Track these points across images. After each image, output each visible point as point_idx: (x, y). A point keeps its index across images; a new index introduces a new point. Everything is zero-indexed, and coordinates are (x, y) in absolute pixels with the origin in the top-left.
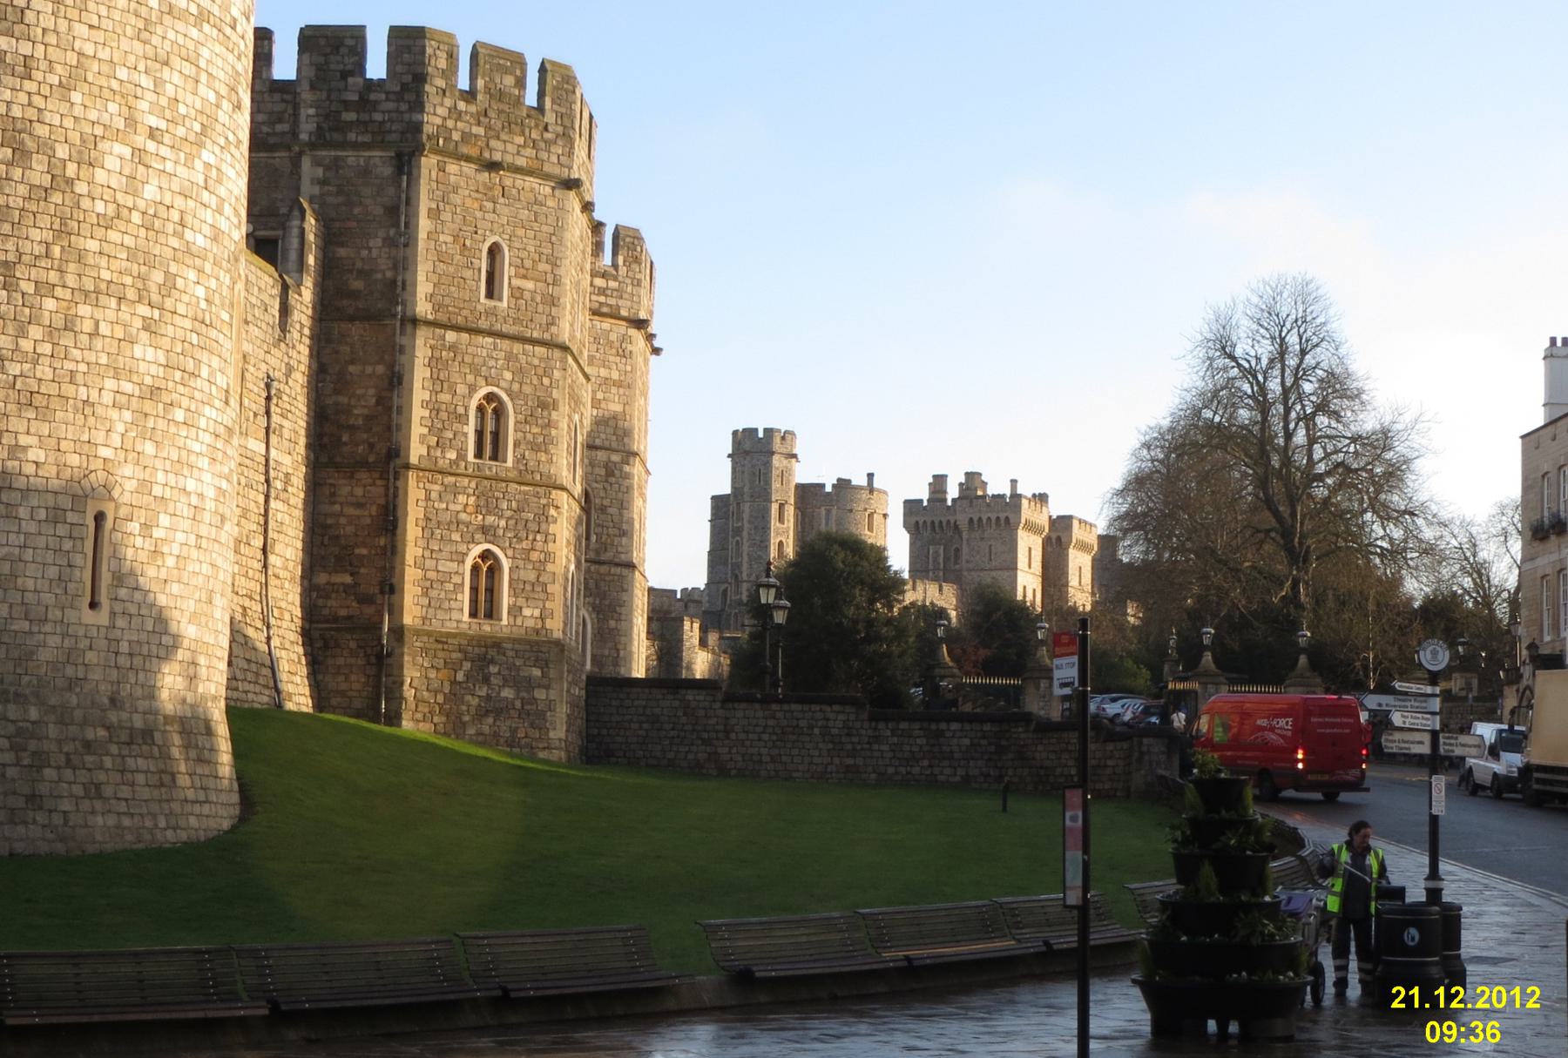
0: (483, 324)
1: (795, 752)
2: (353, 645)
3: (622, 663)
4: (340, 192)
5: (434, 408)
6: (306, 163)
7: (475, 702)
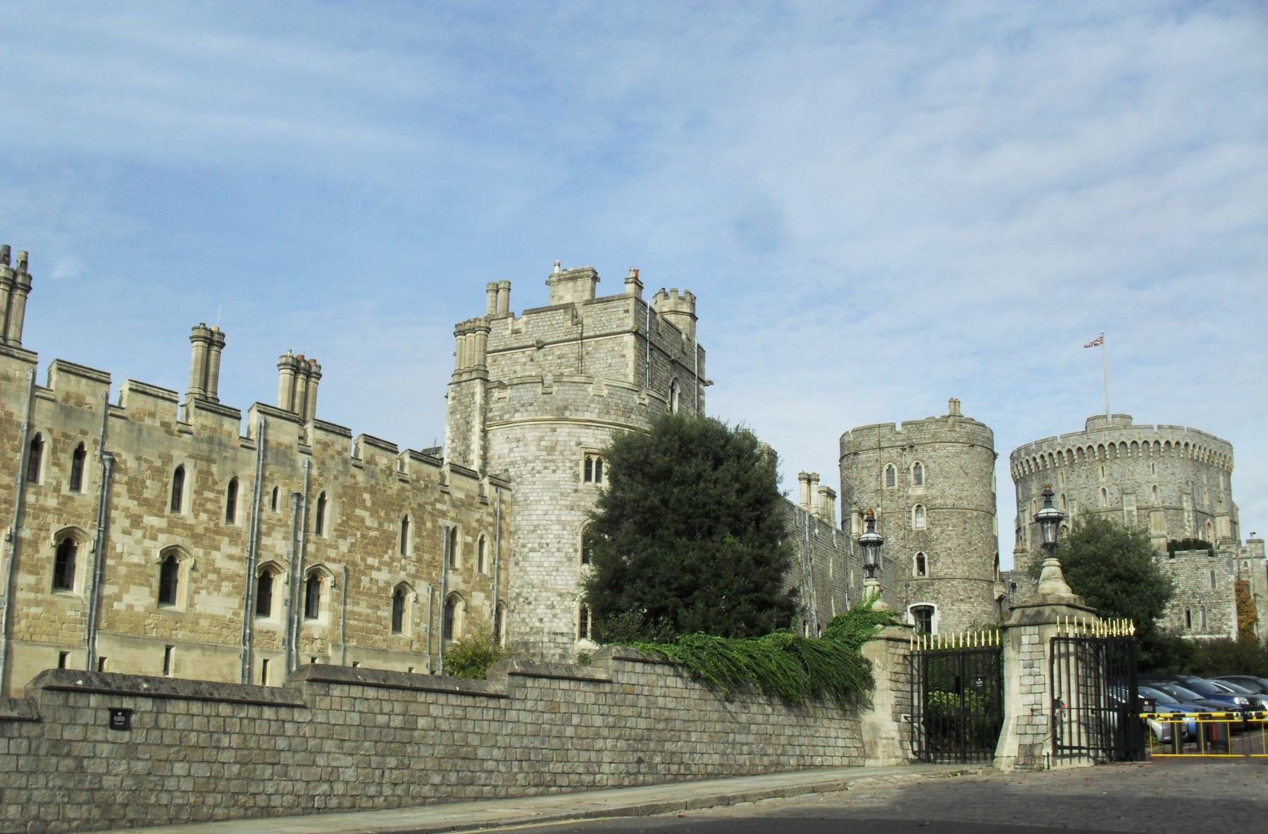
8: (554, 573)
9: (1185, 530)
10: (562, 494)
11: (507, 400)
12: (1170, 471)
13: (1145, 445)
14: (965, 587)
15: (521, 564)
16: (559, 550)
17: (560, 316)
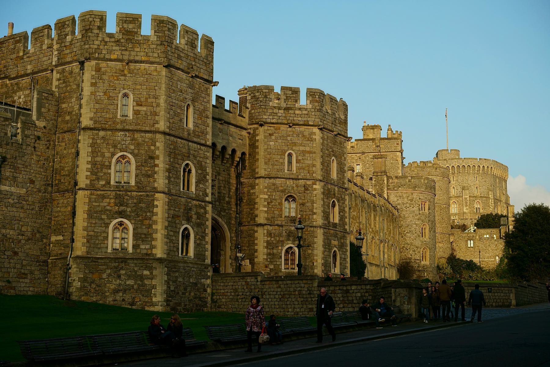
0: (119, 127)
1: (288, 303)
2: (60, 265)
3: (316, 267)
4: (64, 82)
5: (94, 163)
6: (55, 72)
7: (113, 287)
8: (415, 240)
9: (490, 208)
10: (416, 215)
11: (396, 183)
12: (484, 180)
13: (474, 167)
14: (441, 237)
15: (404, 237)
16: (416, 233)
17: (370, 143)
